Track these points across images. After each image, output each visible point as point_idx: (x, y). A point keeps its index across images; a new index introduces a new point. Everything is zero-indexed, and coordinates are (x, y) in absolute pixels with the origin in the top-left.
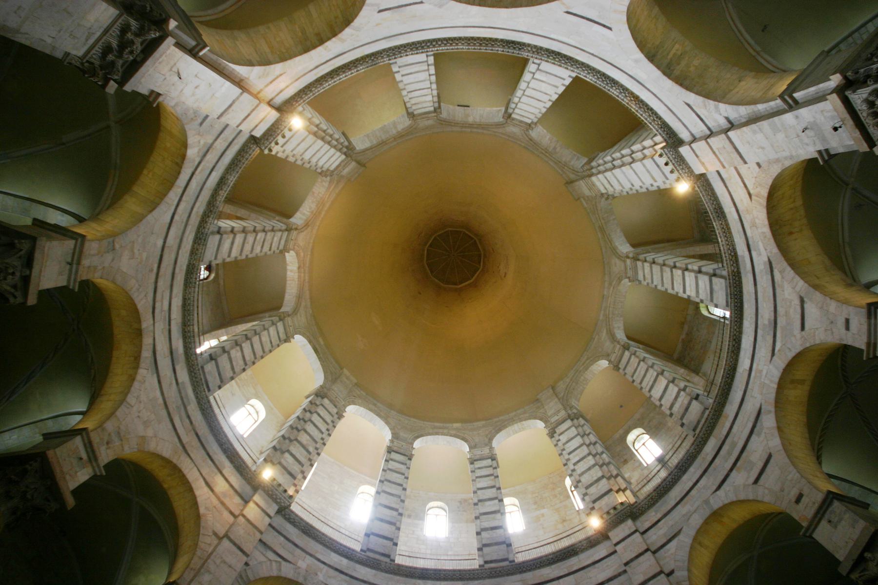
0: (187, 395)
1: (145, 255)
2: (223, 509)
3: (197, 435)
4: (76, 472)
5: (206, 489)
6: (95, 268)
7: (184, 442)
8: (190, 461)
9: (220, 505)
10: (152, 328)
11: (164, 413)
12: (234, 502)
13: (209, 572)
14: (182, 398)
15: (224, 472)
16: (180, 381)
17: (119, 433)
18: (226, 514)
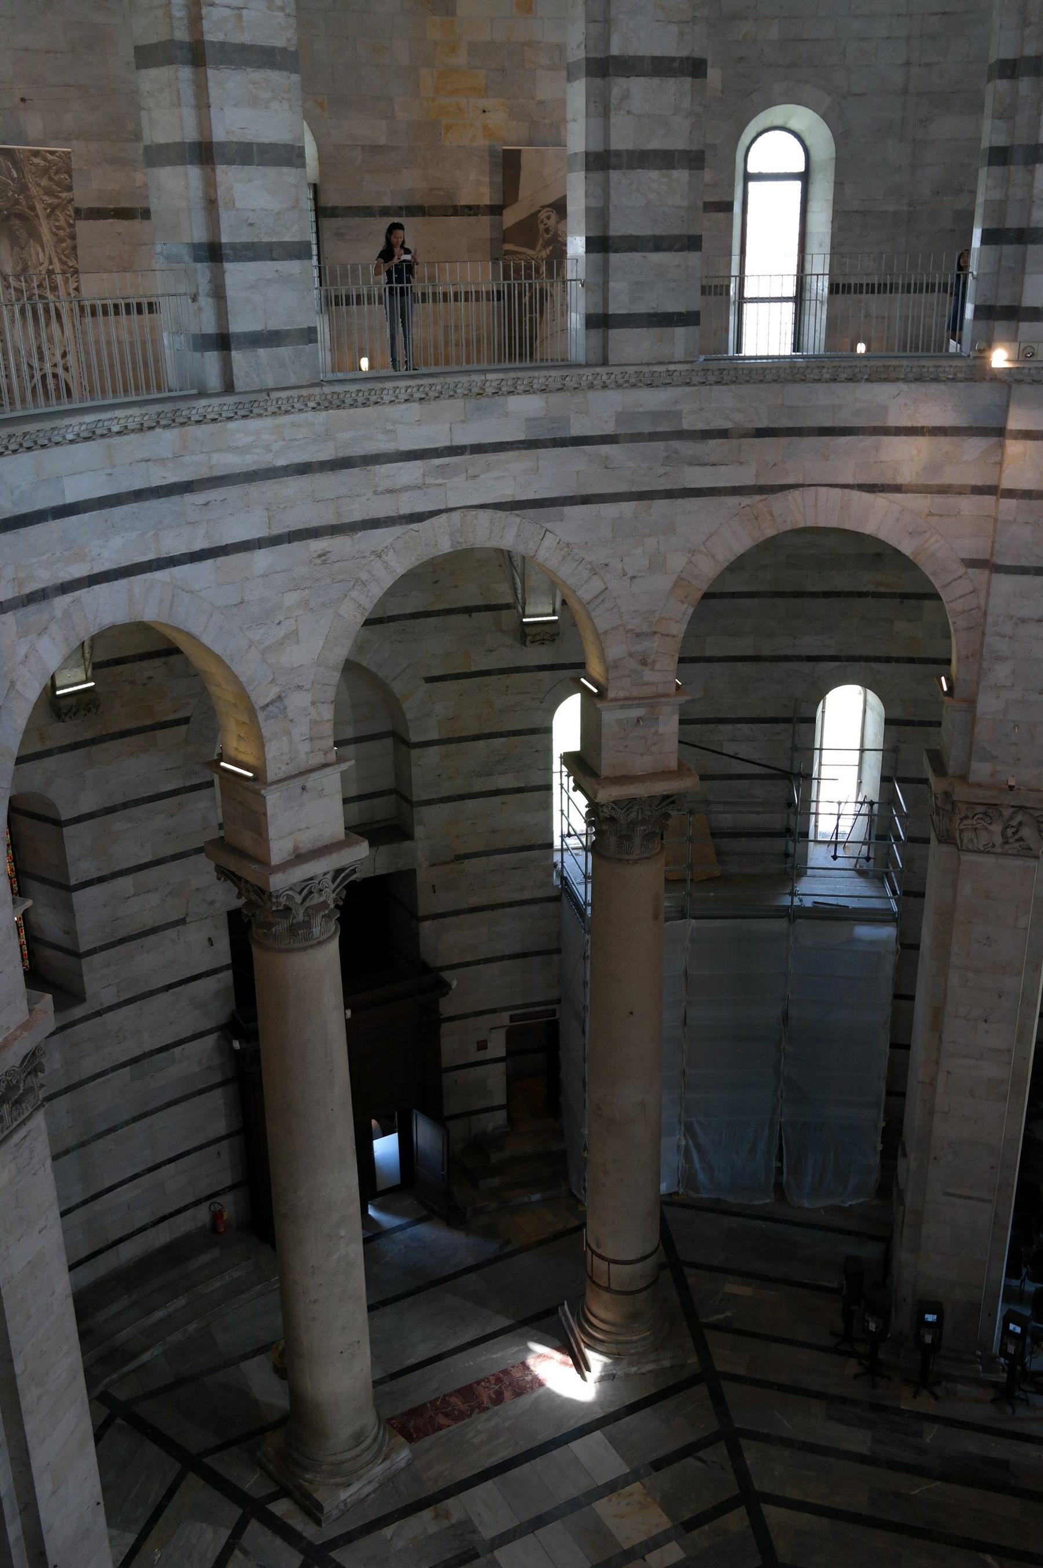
0: (656, 416)
1: (291, 599)
2: (952, 500)
3: (762, 433)
4: (656, 733)
5: (880, 501)
6: (314, 723)
7: (750, 481)
8: (796, 493)
9: (939, 499)
10: (456, 516)
11: (661, 506)
12: (967, 462)
13: (1000, 659)
14: (653, 437)
15: (894, 420)
16: (609, 429)
17: (638, 635)
18: (967, 505)
